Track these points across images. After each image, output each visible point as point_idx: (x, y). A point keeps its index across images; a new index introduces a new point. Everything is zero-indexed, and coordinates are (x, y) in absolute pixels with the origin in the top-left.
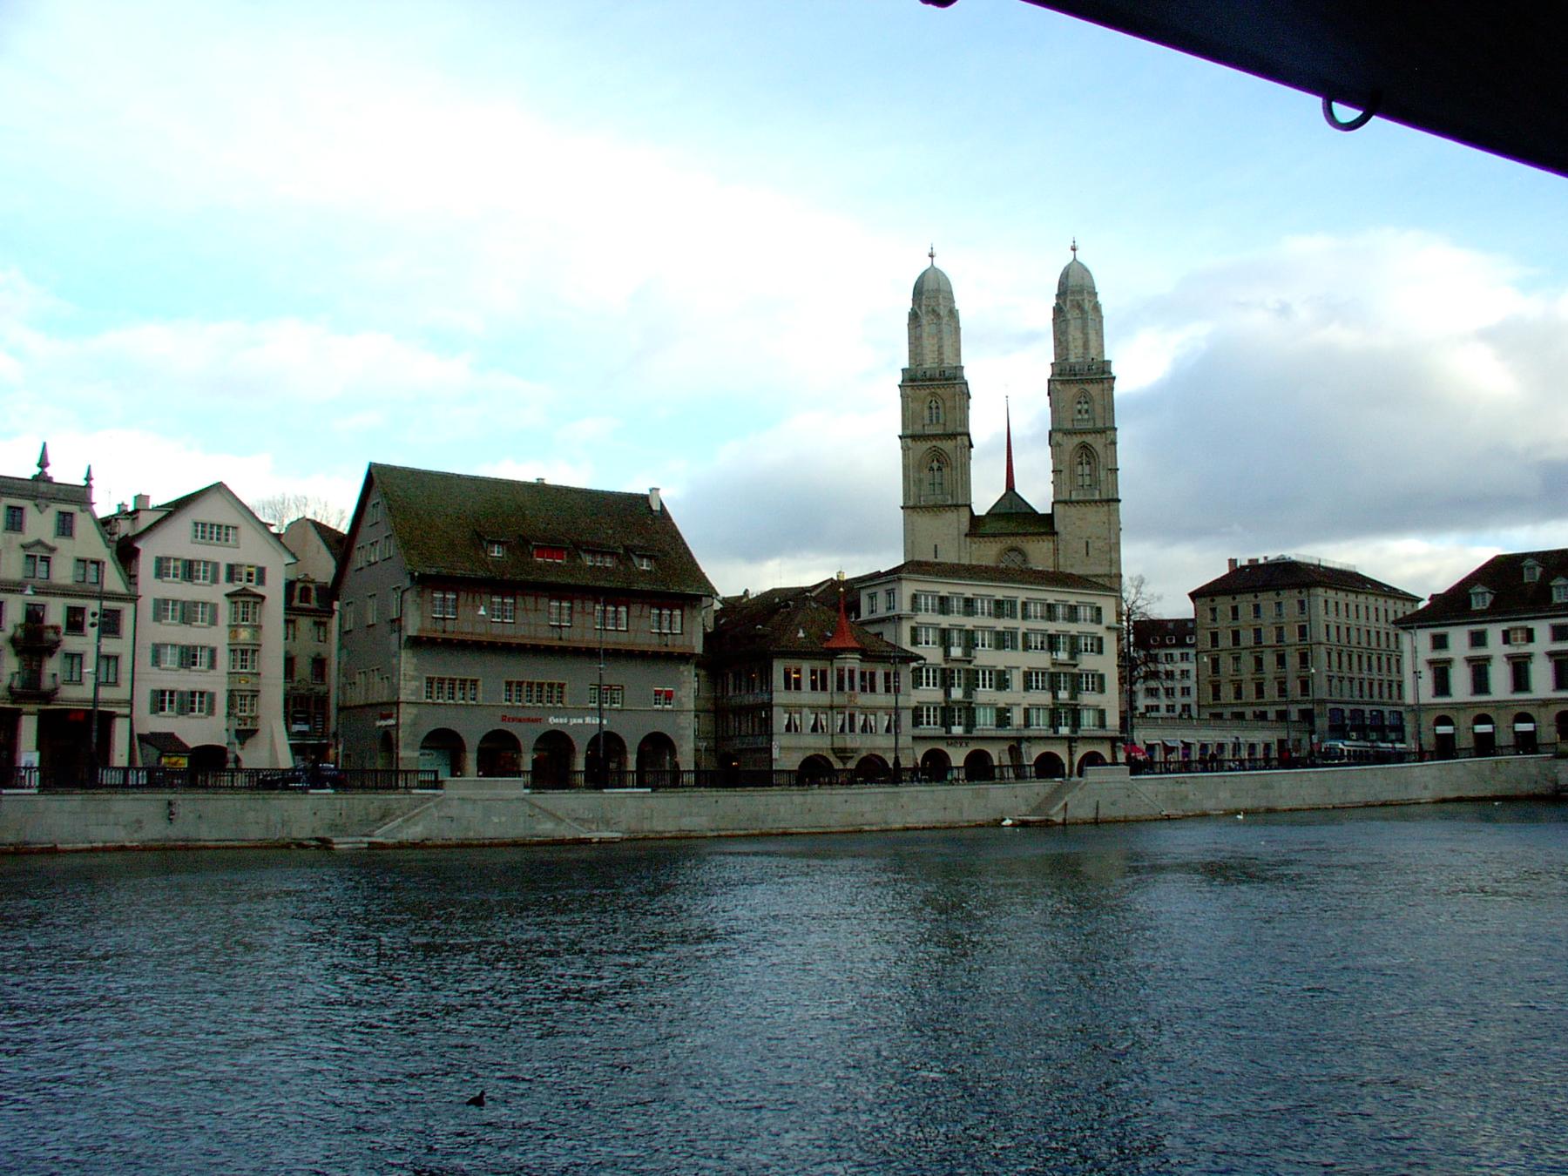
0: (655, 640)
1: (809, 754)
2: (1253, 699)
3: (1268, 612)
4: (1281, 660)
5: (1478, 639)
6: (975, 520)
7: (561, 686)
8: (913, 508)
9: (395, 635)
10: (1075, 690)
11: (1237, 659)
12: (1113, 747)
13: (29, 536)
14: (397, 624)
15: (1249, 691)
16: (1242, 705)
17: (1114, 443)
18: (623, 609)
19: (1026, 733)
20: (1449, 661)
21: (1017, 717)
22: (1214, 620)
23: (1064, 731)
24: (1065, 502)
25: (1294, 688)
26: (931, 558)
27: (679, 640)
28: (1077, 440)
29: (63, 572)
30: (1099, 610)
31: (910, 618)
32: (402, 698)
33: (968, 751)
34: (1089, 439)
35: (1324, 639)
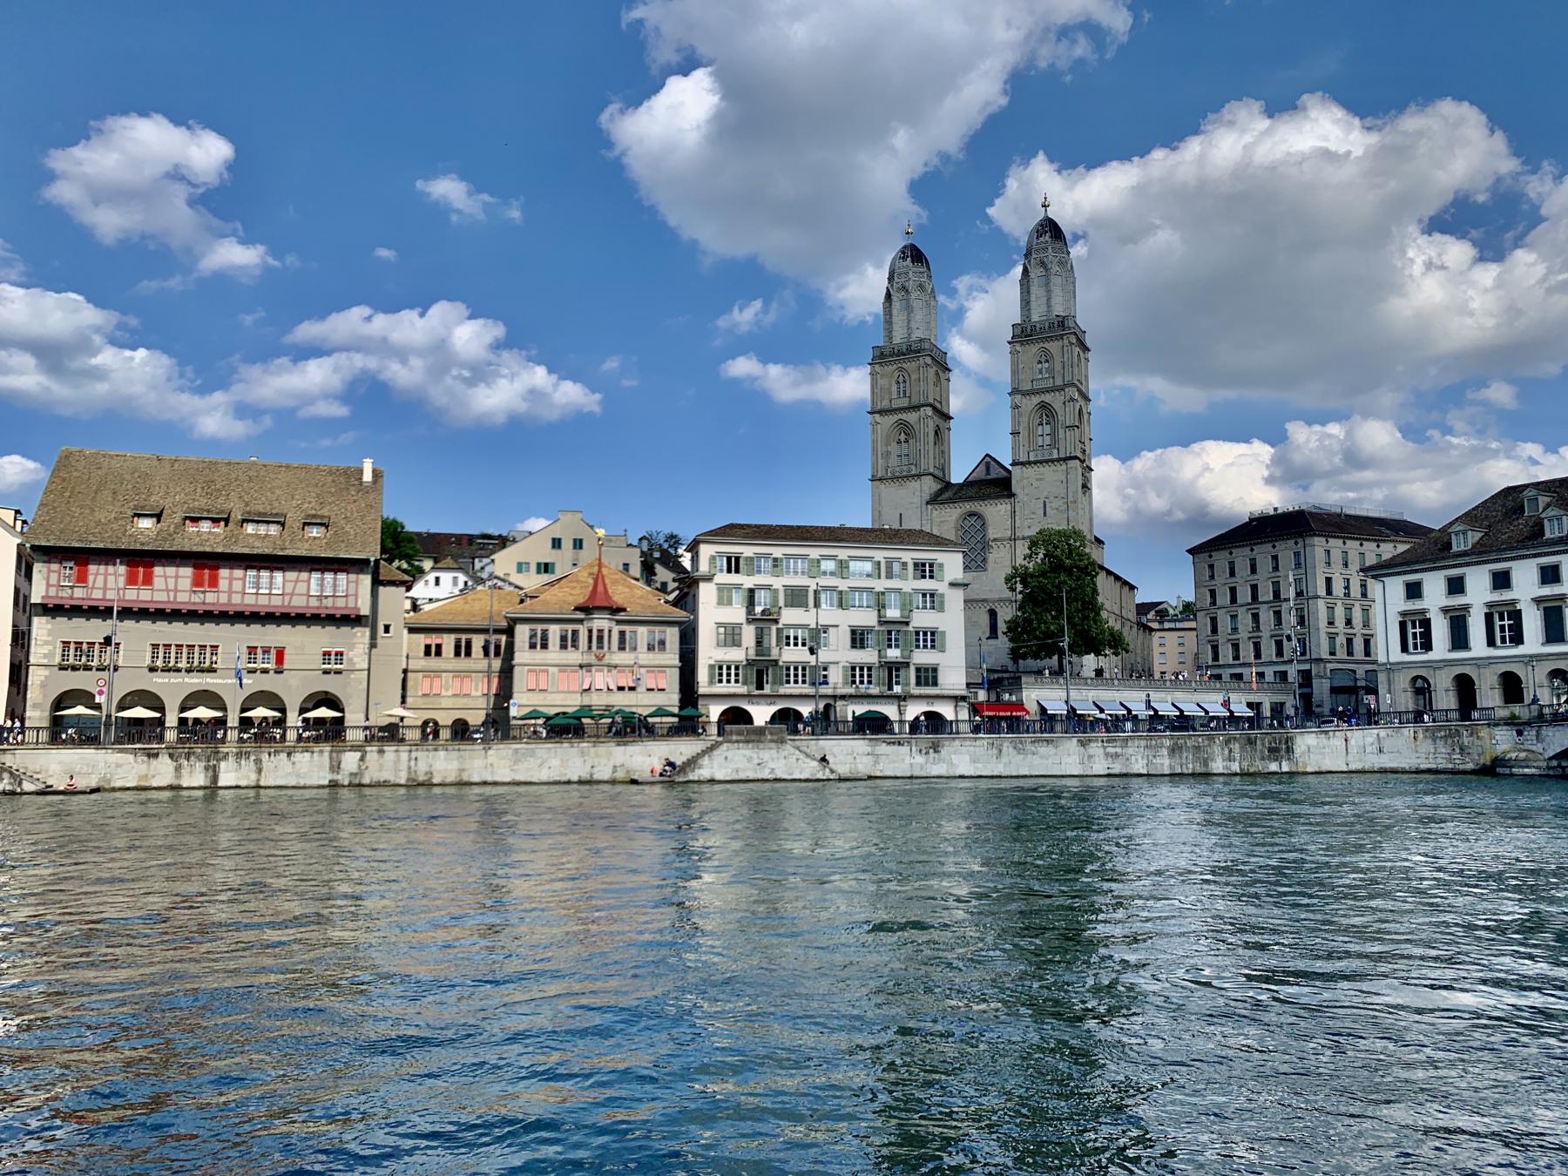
2: (1252, 659)
3: (1264, 565)
5: (1456, 586)
6: (948, 485)
11: (1234, 617)
16: (1285, 663)
21: (836, 677)
22: (1212, 577)
23: (897, 689)
24: (1023, 464)
26: (896, 526)
27: (341, 603)
28: (1036, 400)
30: (941, 565)
31: (709, 579)
32: (32, 660)
33: (774, 709)
34: (1047, 398)
35: (1322, 592)
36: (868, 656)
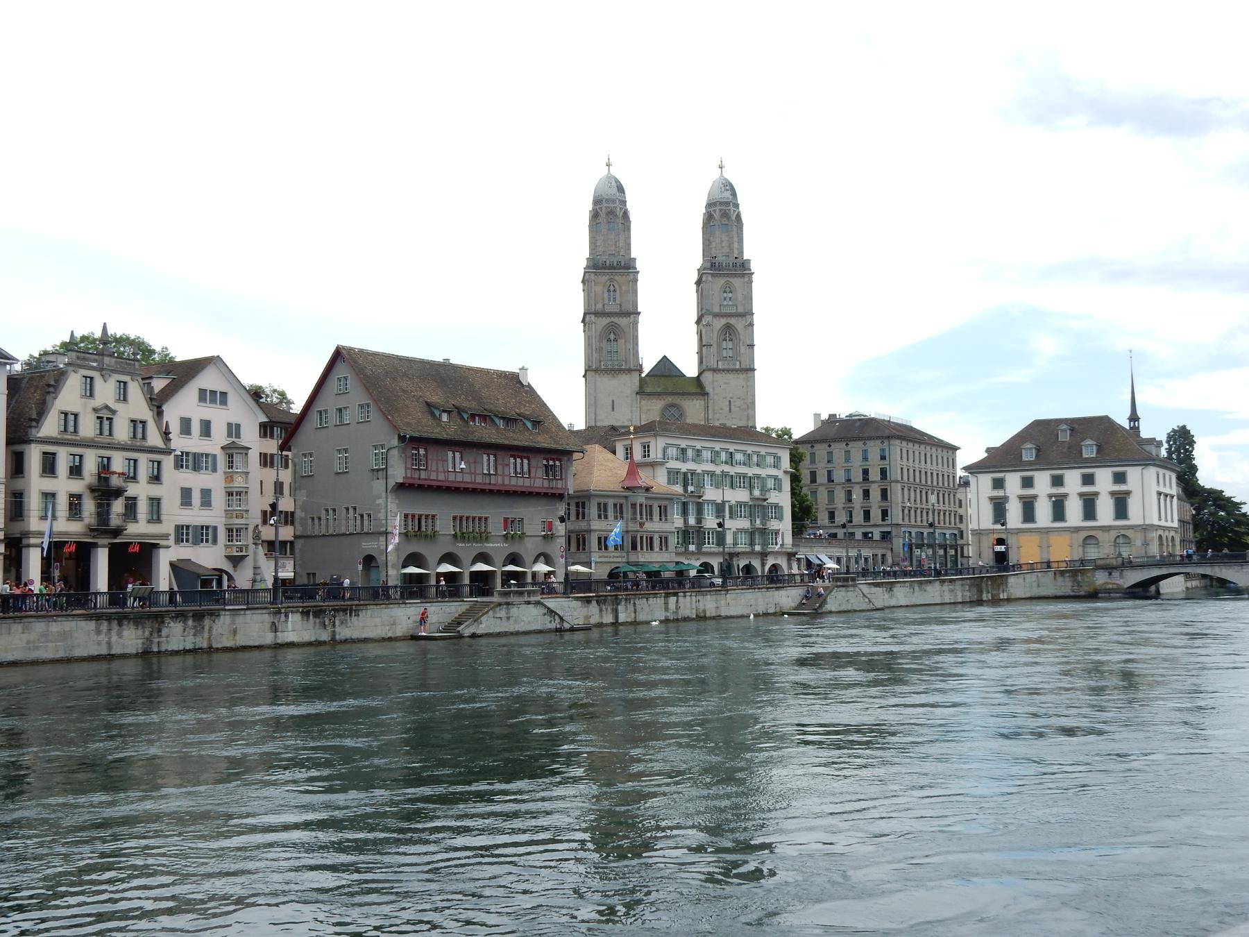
0: (546, 484)
1: (614, 566)
4: (866, 494)
7: (486, 519)
8: (596, 371)
9: (382, 482)
10: (765, 518)
12: (789, 560)
13: (98, 401)
14: (381, 472)
15: (841, 518)
17: (751, 325)
18: (525, 461)
19: (737, 550)
20: (1005, 499)
23: (758, 548)
25: (876, 515)
28: (723, 321)
29: (122, 432)
31: (662, 464)
34: (732, 321)
36: (744, 523)
